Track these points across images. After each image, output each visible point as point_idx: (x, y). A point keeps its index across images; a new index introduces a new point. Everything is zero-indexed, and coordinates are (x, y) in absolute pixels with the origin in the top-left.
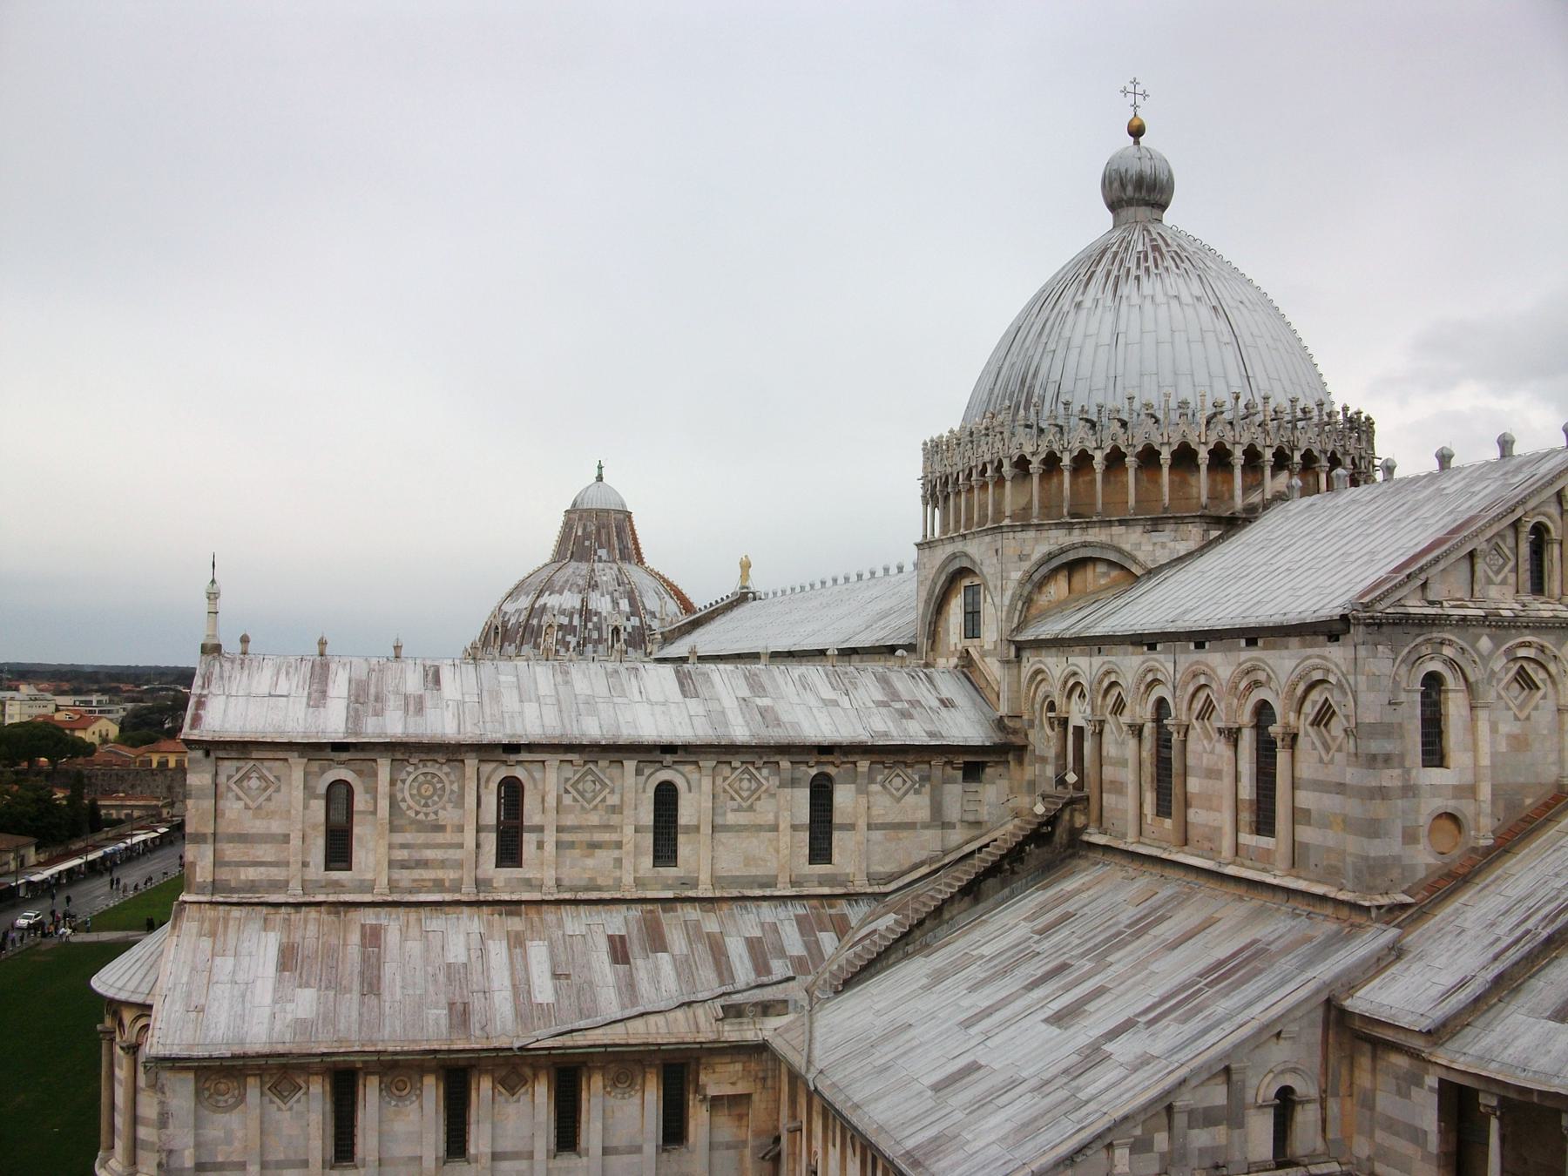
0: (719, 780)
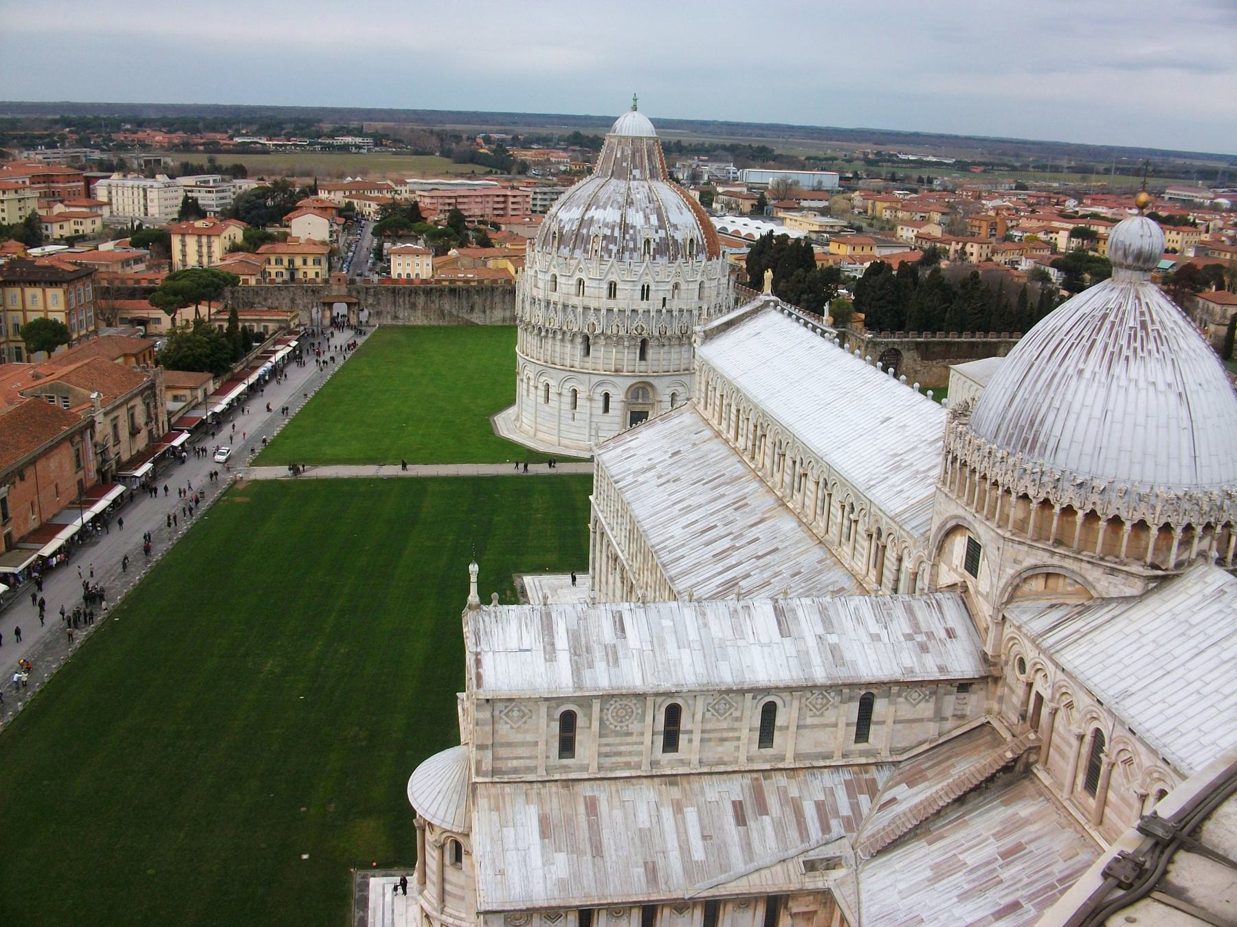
0: (803, 700)
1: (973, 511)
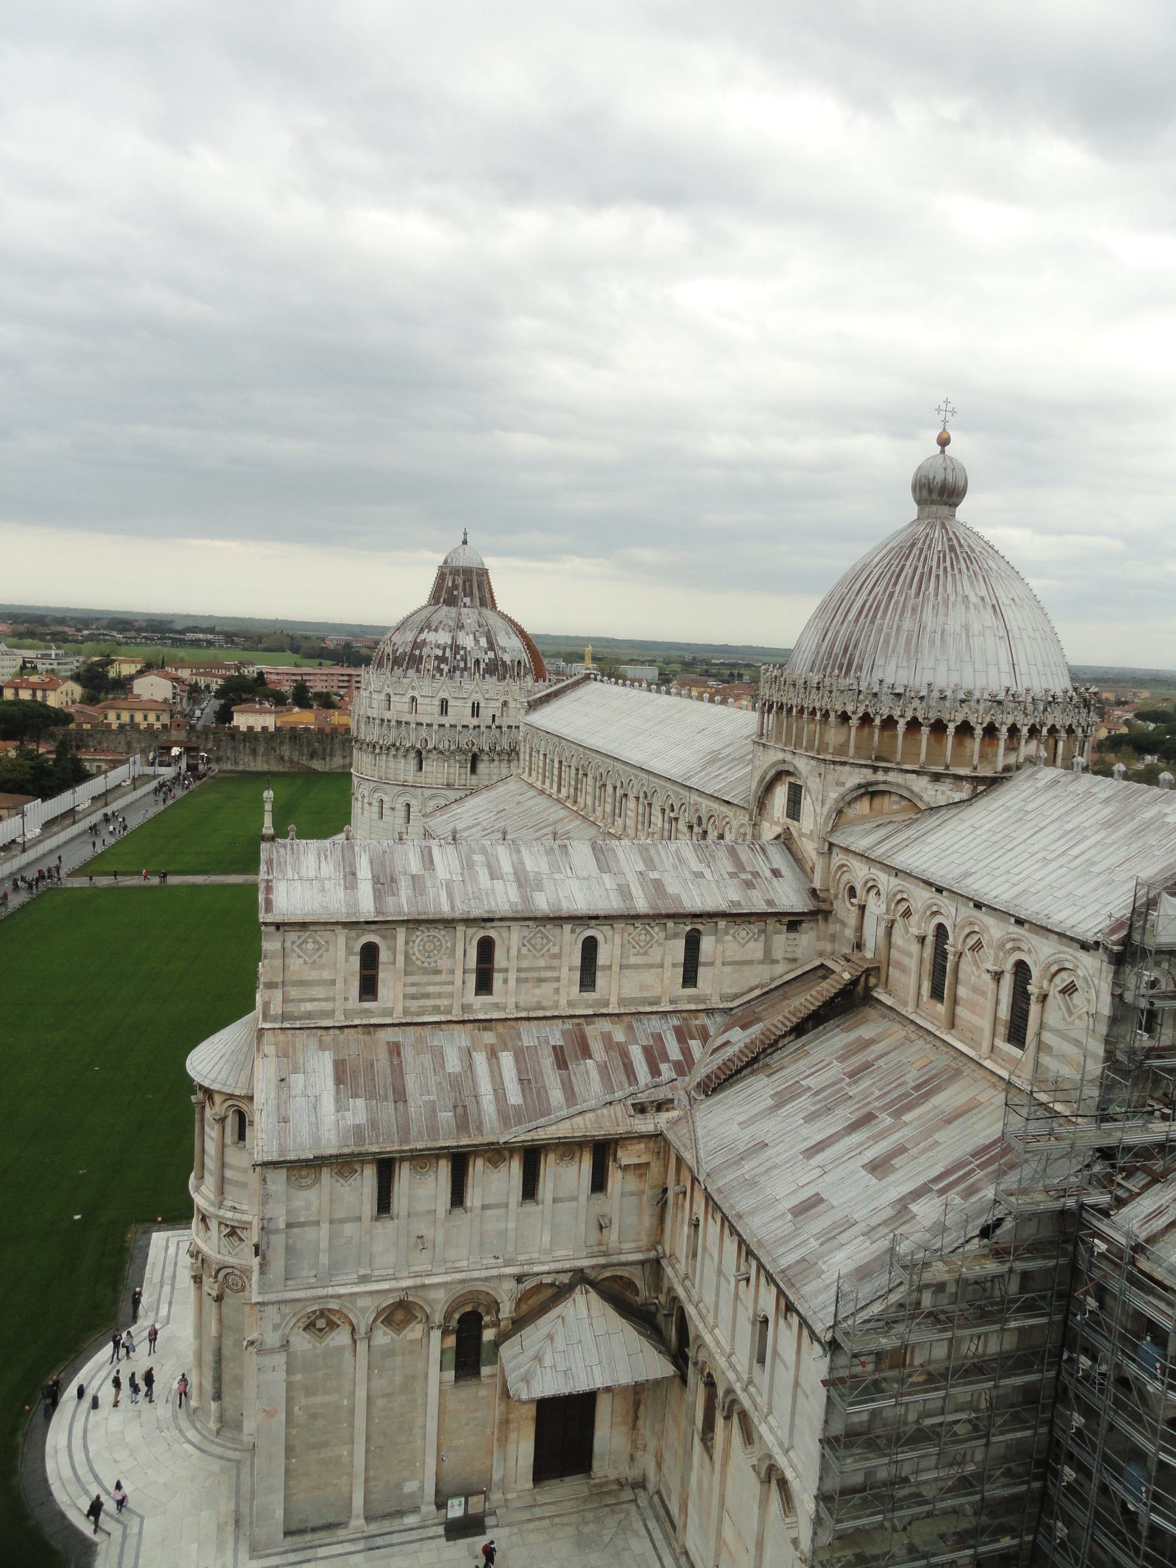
0: (626, 935)
1: (792, 748)
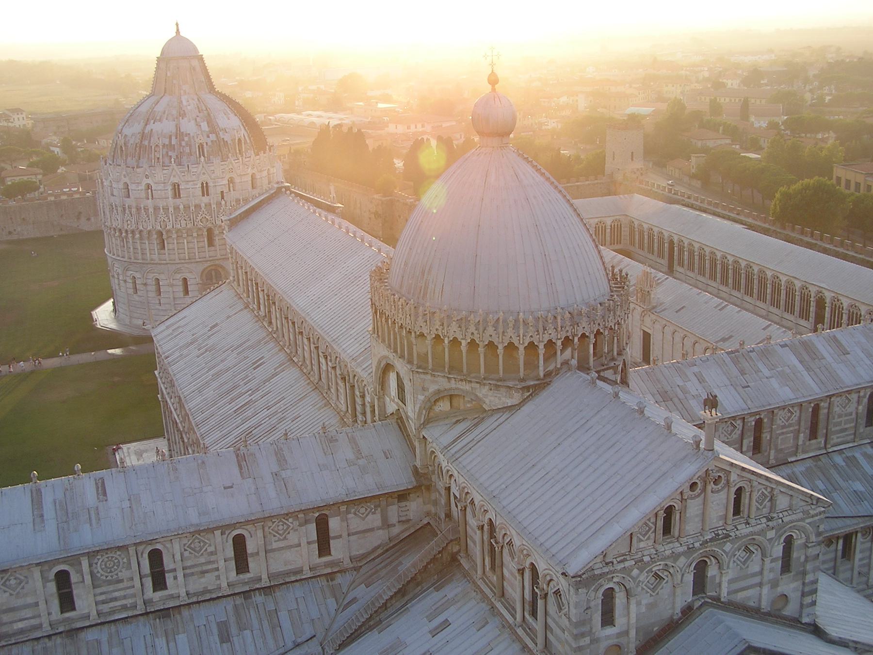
0: (266, 529)
